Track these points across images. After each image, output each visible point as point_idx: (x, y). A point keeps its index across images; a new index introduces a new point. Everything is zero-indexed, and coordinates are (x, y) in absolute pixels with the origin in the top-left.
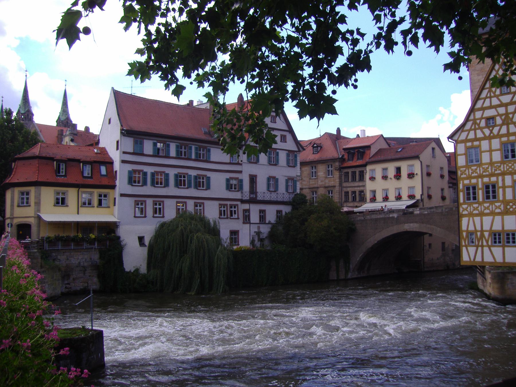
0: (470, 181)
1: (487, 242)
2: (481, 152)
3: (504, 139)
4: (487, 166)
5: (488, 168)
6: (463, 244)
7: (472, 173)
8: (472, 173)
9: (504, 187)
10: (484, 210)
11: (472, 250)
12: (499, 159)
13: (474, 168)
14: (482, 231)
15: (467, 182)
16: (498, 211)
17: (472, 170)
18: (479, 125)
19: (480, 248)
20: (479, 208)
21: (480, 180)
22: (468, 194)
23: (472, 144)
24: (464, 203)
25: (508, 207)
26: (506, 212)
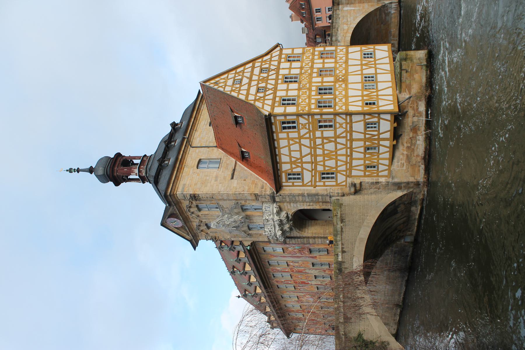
0: (312, 104)
2: (287, 96)
6: (376, 109)
11: (381, 103)
14: (363, 96)
15: (313, 106)
16: (343, 86)
17: (302, 102)
18: (261, 97)
19: (379, 97)
20: (340, 98)
22: (326, 107)
24: (335, 109)
25: (341, 79)
26: (345, 81)
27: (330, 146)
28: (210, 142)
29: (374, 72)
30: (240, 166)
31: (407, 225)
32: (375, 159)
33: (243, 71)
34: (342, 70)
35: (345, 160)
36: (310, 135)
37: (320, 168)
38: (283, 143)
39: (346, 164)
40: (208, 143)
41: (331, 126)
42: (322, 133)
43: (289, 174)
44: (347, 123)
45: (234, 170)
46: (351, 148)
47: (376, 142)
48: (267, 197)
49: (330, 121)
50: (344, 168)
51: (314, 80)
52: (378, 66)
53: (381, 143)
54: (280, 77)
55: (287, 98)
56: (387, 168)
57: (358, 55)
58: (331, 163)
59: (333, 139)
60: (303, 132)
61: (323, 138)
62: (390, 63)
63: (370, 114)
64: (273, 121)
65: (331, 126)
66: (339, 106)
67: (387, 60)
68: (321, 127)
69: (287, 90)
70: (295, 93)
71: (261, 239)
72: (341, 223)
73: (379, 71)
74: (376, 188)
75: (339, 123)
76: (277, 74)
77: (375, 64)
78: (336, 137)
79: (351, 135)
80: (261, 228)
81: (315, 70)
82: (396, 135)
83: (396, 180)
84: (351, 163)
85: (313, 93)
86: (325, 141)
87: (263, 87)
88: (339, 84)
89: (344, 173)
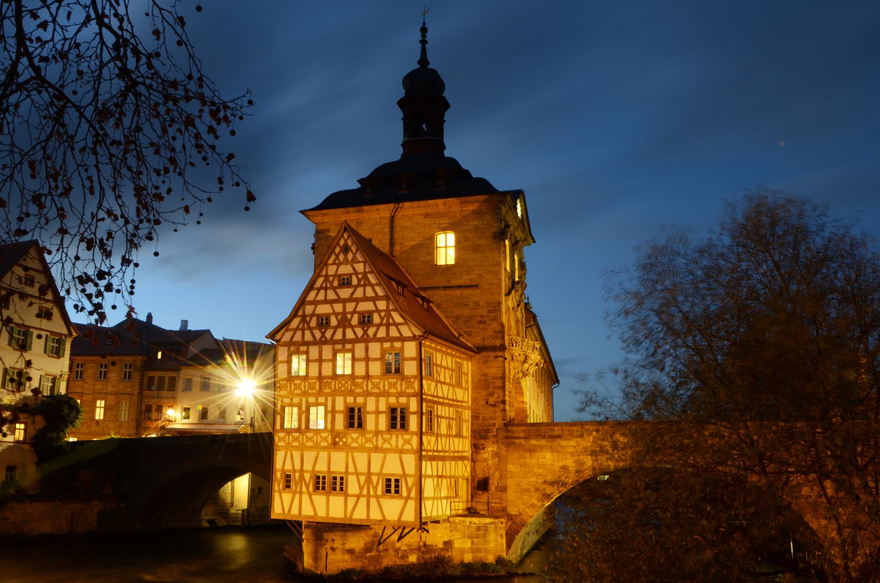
1: (308, 488)
6: (276, 488)
11: (287, 497)
16: (324, 444)
18: (308, 324)
19: (297, 496)
25: (337, 440)
28: (402, 244)
29: (349, 492)
33: (368, 283)
40: (402, 241)
52: (363, 501)
57: (392, 468)
67: (375, 515)
73: (351, 501)
77: (368, 496)
81: (360, 400)
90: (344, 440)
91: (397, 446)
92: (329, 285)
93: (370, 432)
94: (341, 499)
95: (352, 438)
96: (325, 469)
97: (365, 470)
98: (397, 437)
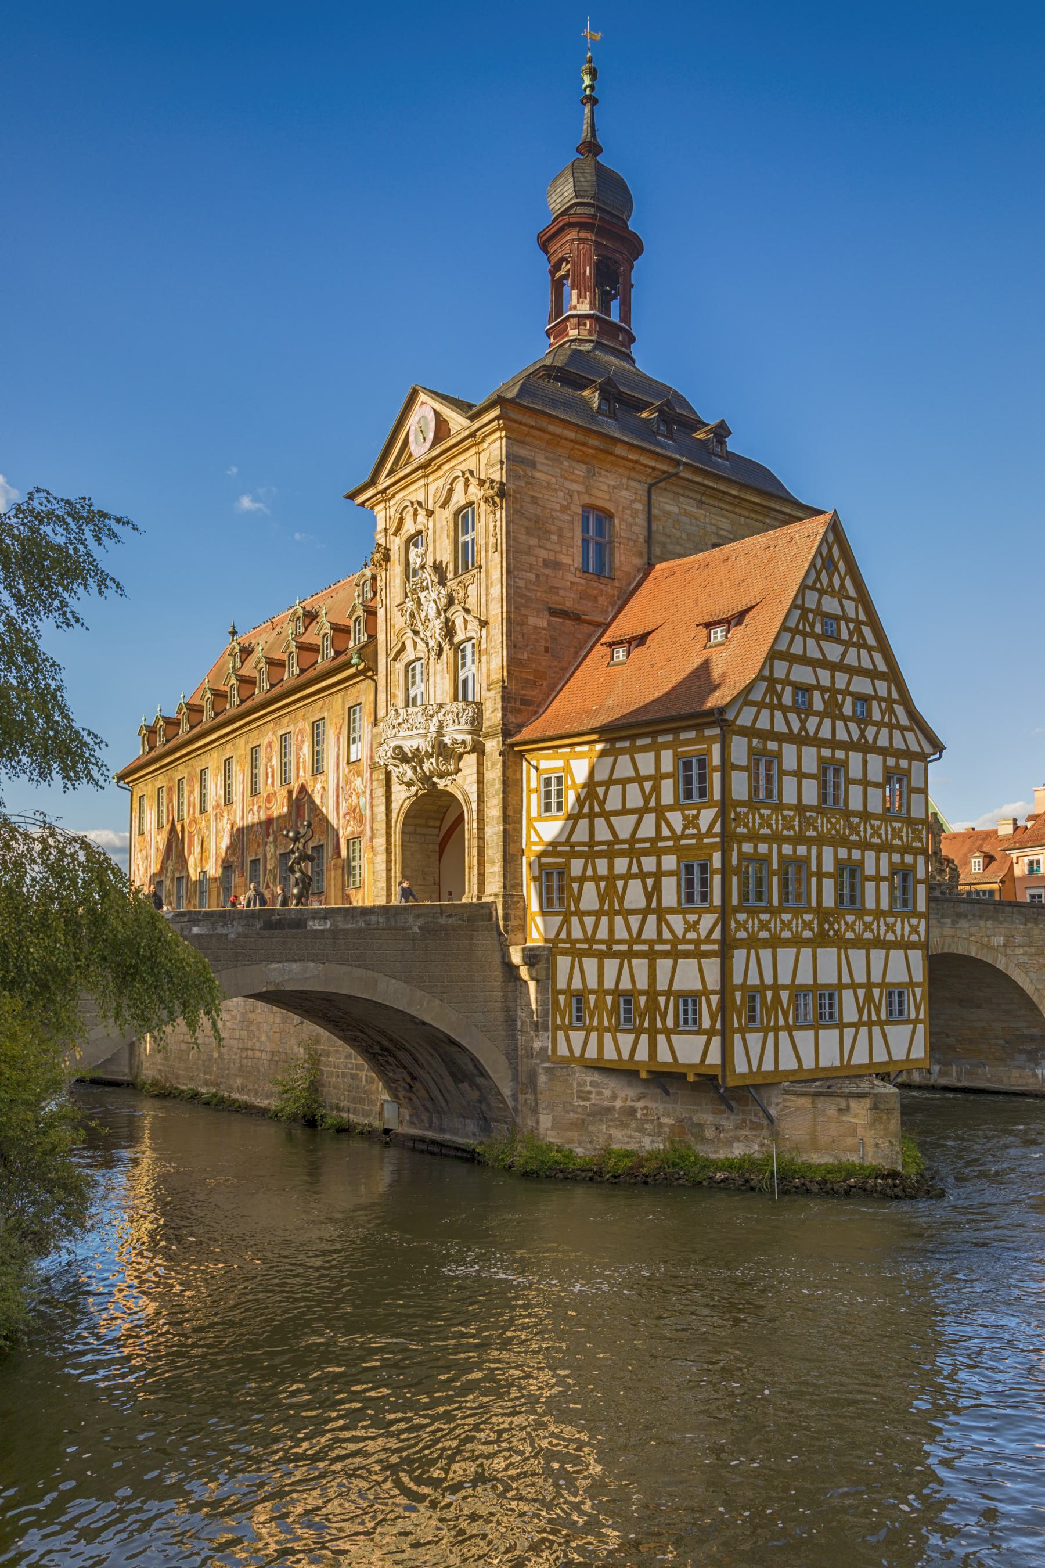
0: (756, 847)
2: (782, 773)
3: (826, 752)
4: (791, 813)
5: (793, 819)
6: (736, 1025)
7: (761, 826)
8: (761, 826)
9: (820, 875)
10: (782, 929)
11: (754, 1039)
12: (815, 803)
13: (766, 812)
14: (776, 987)
15: (747, 848)
16: (807, 934)
17: (761, 816)
19: (771, 1035)
21: (775, 847)
23: (765, 745)
25: (826, 926)
26: (822, 940)
27: (635, 895)
28: (664, 545)
30: (590, 636)
31: (427, 1109)
32: (601, 1021)
34: (853, 930)
35: (598, 936)
36: (667, 839)
37: (576, 867)
38: (646, 763)
39: (586, 941)
41: (690, 898)
42: (670, 873)
43: (559, 780)
44: (697, 942)
45: (577, 618)
46: (631, 954)
47: (646, 1025)
48: (500, 715)
49: (704, 897)
50: (577, 933)
51: (828, 852)
52: (864, 1030)
53: (644, 1038)
54: (840, 754)
55: (775, 772)
56: (577, 1053)
57: (897, 974)
58: (589, 898)
59: (654, 905)
60: (676, 819)
61: (659, 874)
62: (871, 1064)
63: (723, 1006)
64: (708, 732)
65: (690, 898)
66: (746, 922)
67: (880, 1056)
68: (689, 869)
69: (799, 774)
70: (790, 797)
71: (382, 697)
72: (420, 928)
73: (849, 1033)
74: (523, 1023)
75: (697, 922)
76: (849, 746)
77: (870, 1024)
78: (661, 913)
79: (665, 954)
80: (415, 698)
81: (856, 855)
82: (665, 1080)
83: (542, 1078)
84: (590, 953)
85: (787, 849)
86: (650, 882)
87: (811, 704)
88: (811, 922)
89: (563, 935)
90: (836, 927)
91: (903, 935)
92: (808, 629)
93: (869, 913)
94: (836, 1032)
95: (846, 923)
96: (811, 982)
97: (864, 980)
98: (903, 923)
